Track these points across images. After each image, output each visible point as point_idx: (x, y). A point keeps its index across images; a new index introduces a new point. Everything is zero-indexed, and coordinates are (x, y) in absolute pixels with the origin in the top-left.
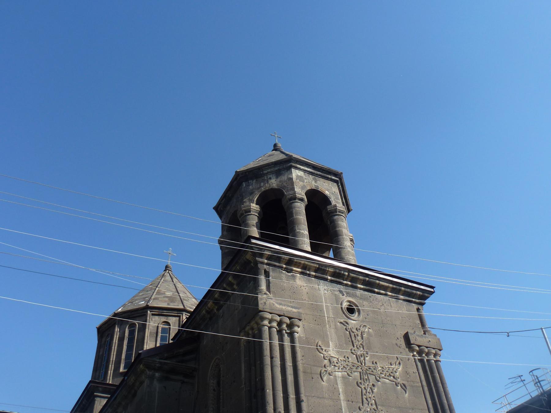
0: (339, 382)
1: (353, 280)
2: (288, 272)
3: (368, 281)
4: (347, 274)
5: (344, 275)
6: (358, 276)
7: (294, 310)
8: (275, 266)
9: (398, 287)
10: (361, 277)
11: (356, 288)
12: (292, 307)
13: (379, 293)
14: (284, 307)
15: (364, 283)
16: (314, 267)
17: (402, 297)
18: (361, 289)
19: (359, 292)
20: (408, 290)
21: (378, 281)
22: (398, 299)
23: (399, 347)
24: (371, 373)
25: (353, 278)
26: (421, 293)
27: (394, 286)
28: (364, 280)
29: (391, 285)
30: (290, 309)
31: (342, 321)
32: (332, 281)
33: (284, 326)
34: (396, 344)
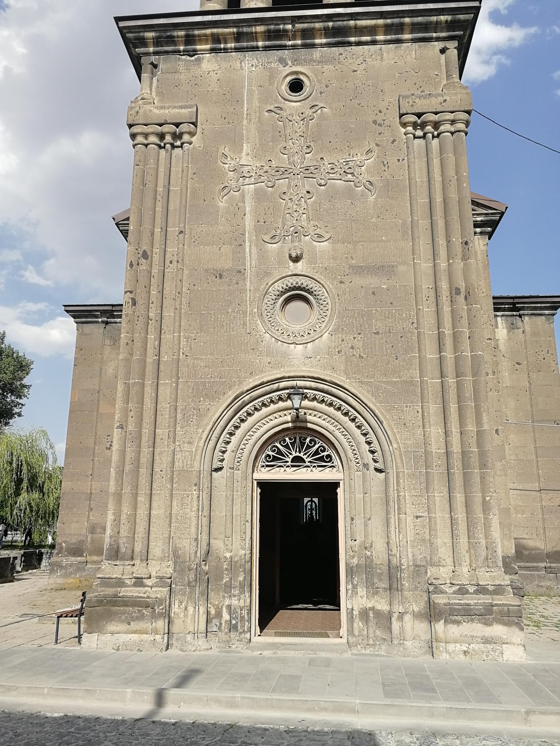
0: (248, 199)
1: (307, 34)
2: (191, 56)
3: (333, 28)
4: (289, 27)
5: (286, 31)
6: (312, 25)
7: (183, 111)
8: (167, 52)
9: (396, 21)
10: (318, 25)
11: (313, 46)
12: (181, 107)
13: (359, 44)
14: (167, 111)
15: (327, 32)
16: (230, 34)
17: (380, 38)
18: (322, 45)
19: (317, 53)
20: (420, 19)
21: (352, 23)
22: (399, 41)
23: (380, 125)
24: (311, 175)
25: (304, 31)
26: (449, 18)
27: (389, 21)
28: (326, 29)
29: (381, 22)
30: (177, 110)
31: (272, 108)
32: (266, 48)
33: (168, 138)
34: (375, 122)
